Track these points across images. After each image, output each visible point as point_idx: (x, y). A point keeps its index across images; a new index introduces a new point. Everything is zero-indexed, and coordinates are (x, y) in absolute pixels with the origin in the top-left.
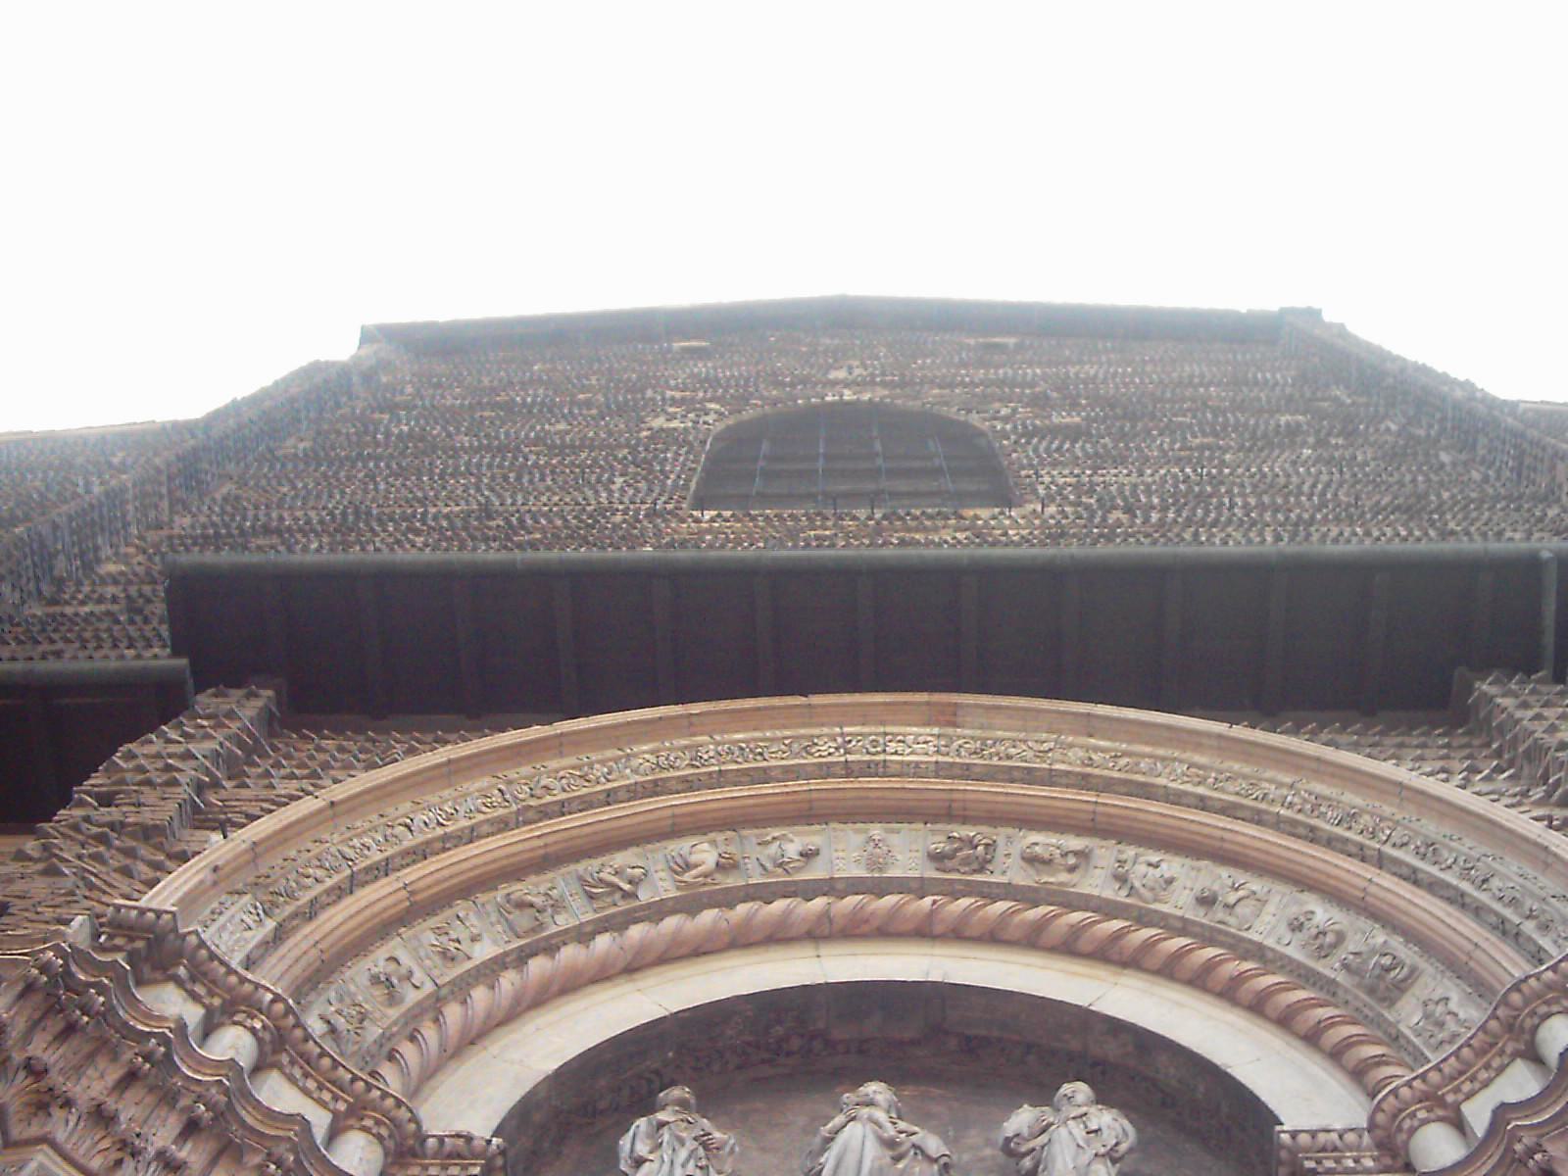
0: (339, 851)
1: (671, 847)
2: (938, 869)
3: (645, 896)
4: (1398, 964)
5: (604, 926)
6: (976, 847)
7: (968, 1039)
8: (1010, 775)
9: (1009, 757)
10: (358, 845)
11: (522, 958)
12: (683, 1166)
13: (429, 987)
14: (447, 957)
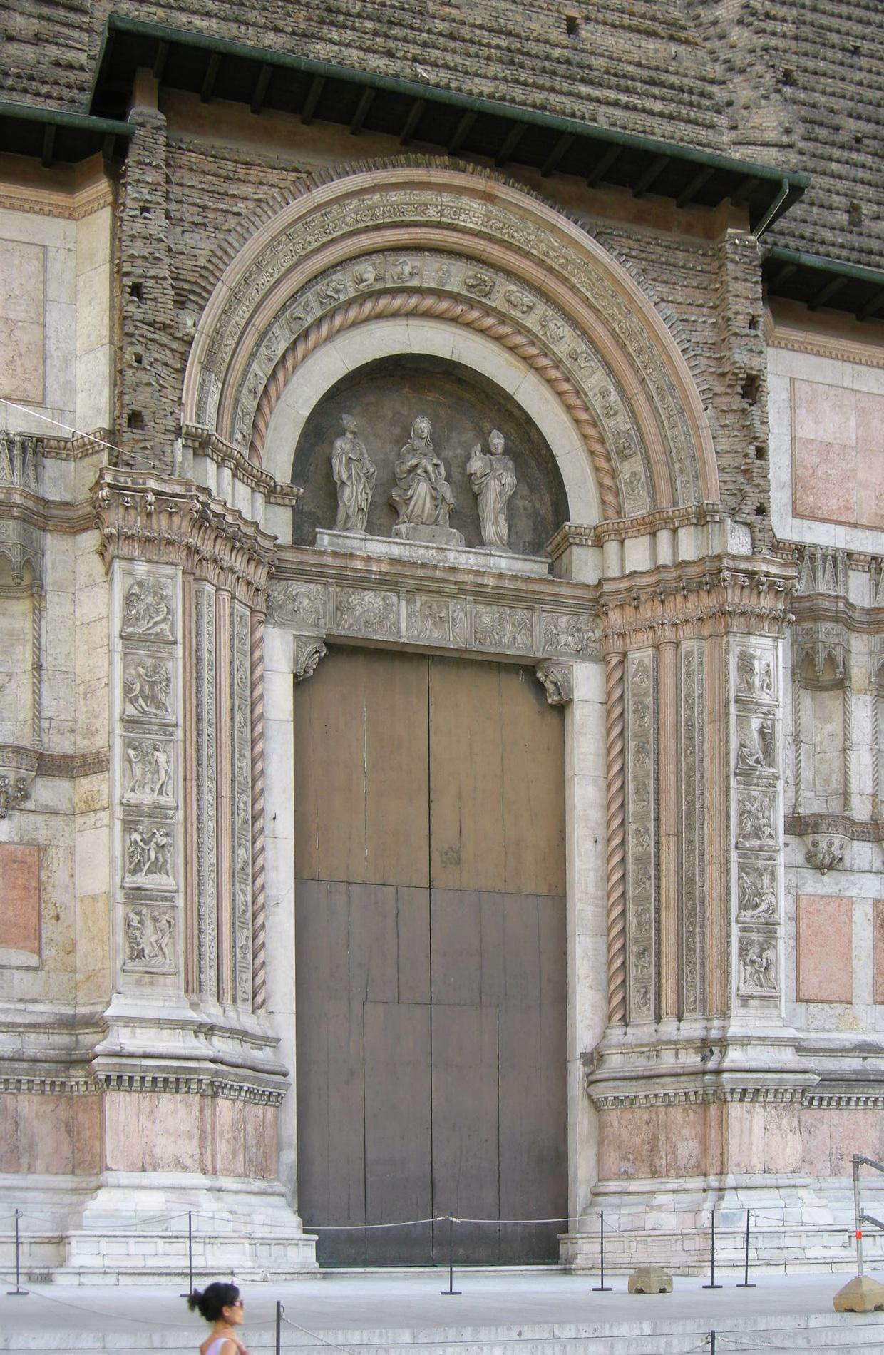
3: (343, 298)
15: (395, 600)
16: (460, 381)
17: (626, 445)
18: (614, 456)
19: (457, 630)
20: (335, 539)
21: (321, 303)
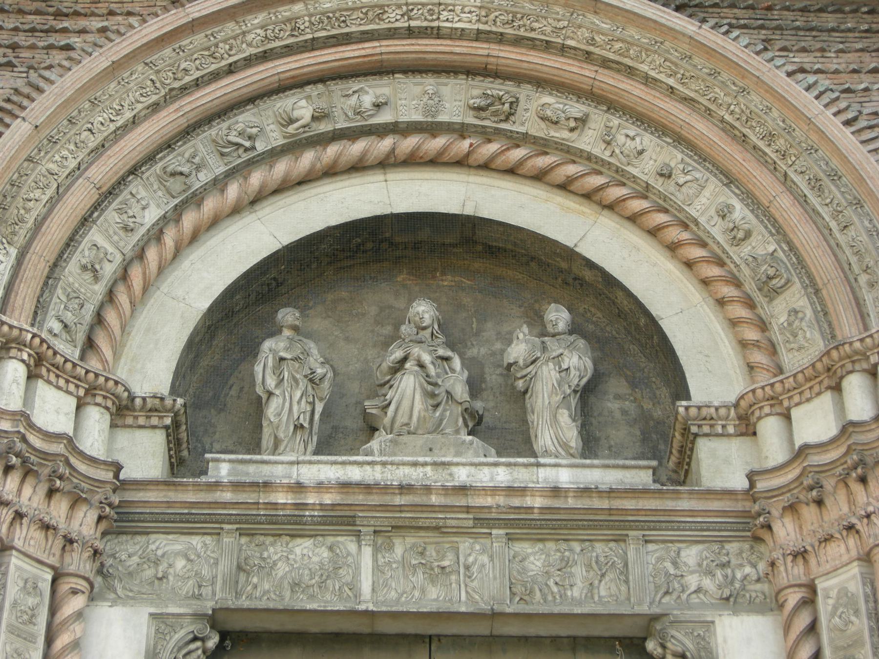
0: (47, 170)
1: (278, 105)
2: (476, 117)
4: (779, 276)
5: (230, 174)
6: (504, 104)
7: (490, 247)
8: (532, 44)
9: (533, 30)
10: (60, 159)
11: (178, 212)
12: (299, 402)
13: (119, 258)
14: (127, 229)
15: (352, 547)
16: (492, 252)
17: (771, 272)
18: (759, 298)
19: (475, 584)
20: (240, 467)
21: (222, 154)
